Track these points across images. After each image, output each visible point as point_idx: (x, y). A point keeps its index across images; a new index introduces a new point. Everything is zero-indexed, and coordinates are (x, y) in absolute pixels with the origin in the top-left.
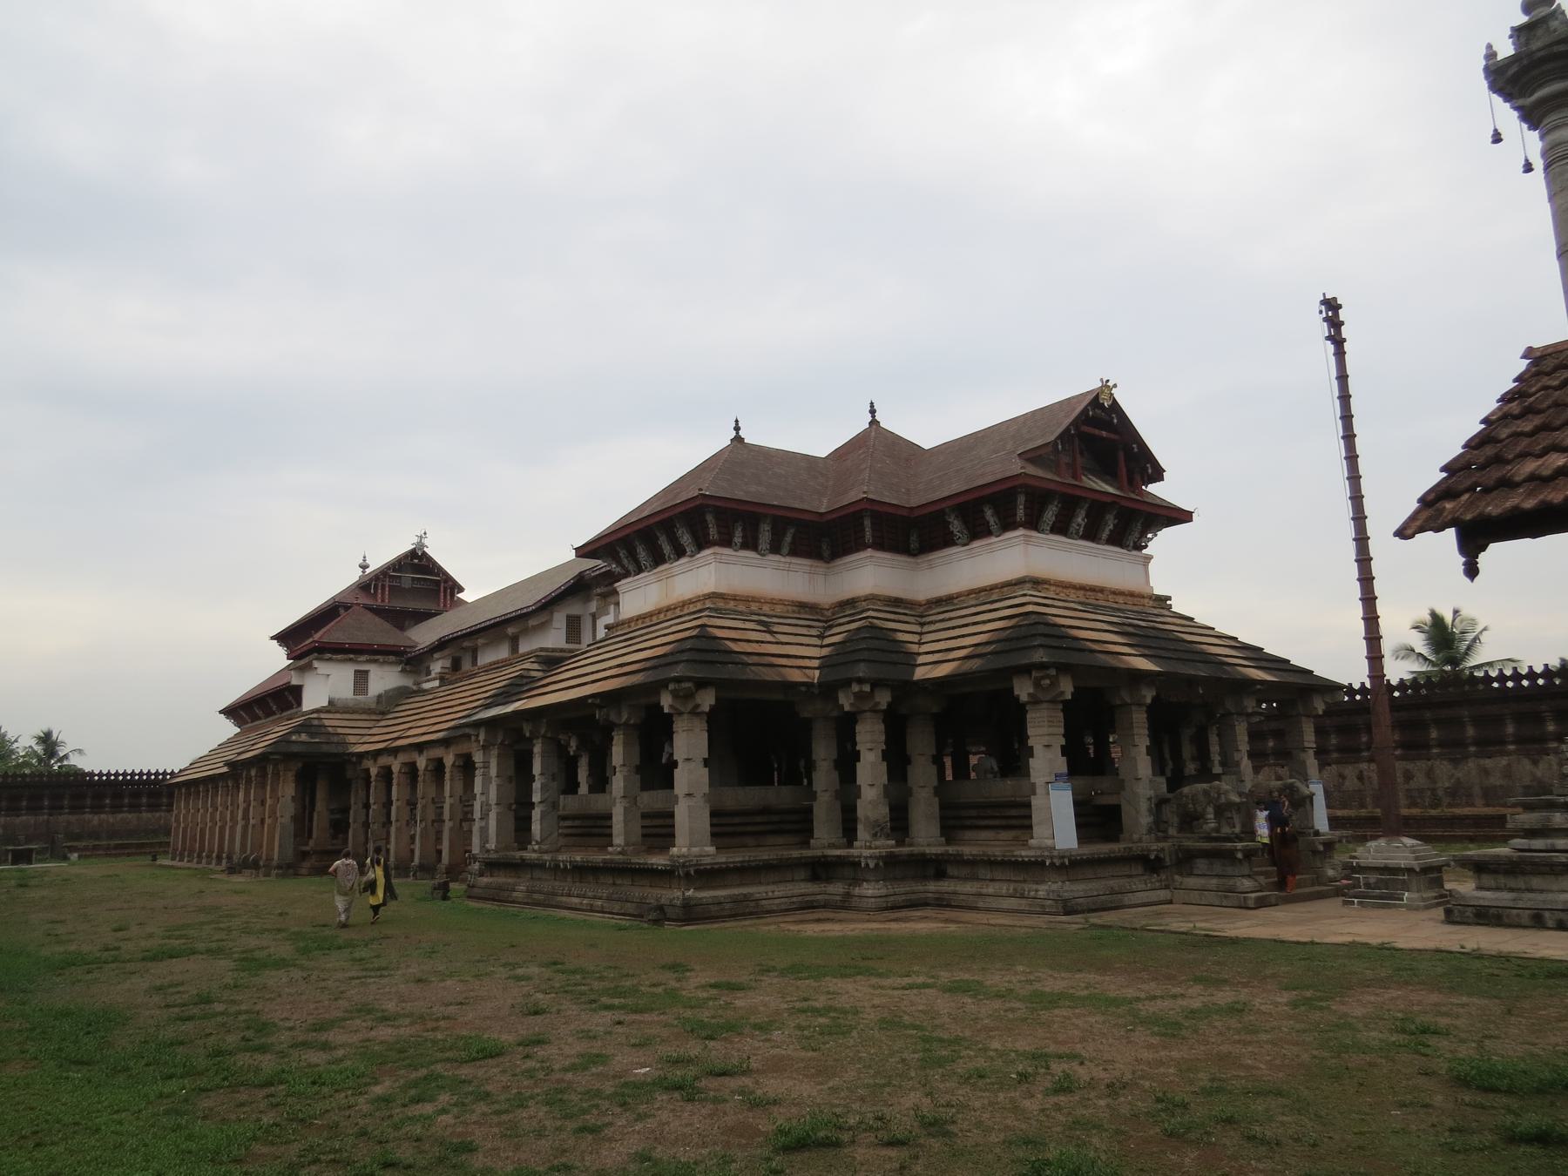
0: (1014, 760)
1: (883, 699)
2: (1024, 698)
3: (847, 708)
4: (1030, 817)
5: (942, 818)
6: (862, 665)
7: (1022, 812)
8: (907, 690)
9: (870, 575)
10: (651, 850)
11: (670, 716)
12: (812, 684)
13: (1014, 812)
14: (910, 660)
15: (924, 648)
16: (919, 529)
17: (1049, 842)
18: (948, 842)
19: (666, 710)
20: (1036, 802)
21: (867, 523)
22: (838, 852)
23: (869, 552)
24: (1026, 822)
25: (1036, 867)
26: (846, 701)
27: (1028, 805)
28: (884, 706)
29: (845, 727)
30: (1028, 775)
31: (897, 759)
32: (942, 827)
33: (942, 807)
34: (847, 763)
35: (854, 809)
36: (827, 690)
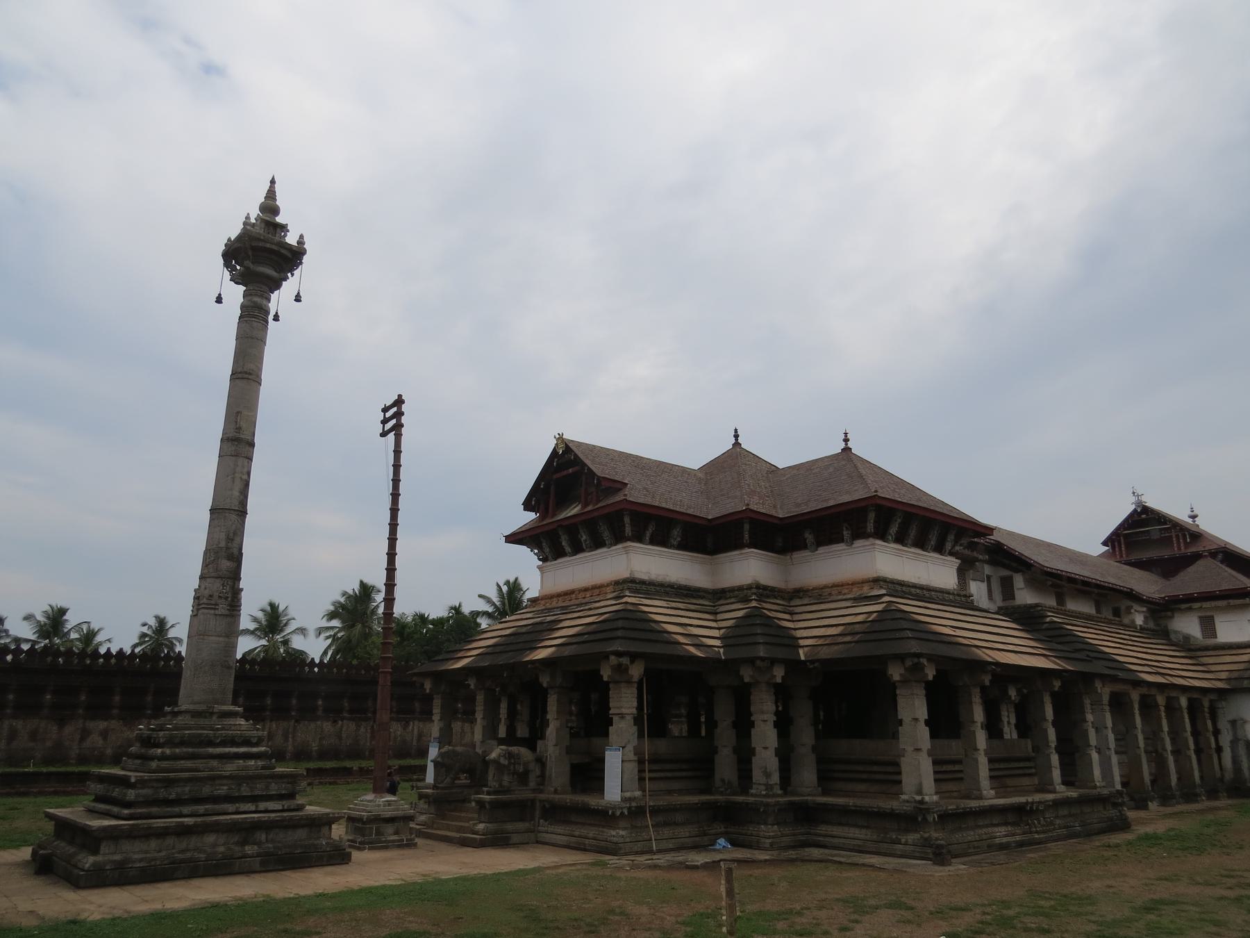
0: (888, 726)
1: (779, 673)
2: (896, 677)
3: (747, 680)
4: (900, 773)
5: (819, 771)
6: (761, 647)
7: (890, 769)
8: (794, 666)
9: (749, 567)
10: (585, 791)
11: (607, 683)
12: (719, 660)
13: (875, 768)
14: (793, 643)
15: (799, 634)
16: (784, 534)
17: (918, 798)
18: (824, 793)
19: (605, 679)
20: (906, 764)
21: (747, 527)
22: (740, 799)
23: (747, 550)
24: (896, 777)
25: (914, 818)
26: (747, 674)
27: (897, 765)
28: (779, 680)
29: (742, 697)
30: (895, 736)
31: (783, 724)
32: (819, 779)
33: (820, 761)
34: (743, 725)
35: (750, 762)
36: (727, 666)
